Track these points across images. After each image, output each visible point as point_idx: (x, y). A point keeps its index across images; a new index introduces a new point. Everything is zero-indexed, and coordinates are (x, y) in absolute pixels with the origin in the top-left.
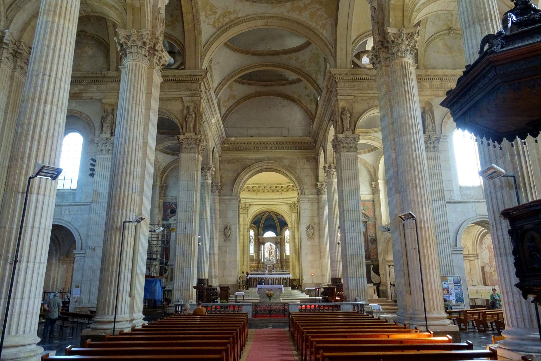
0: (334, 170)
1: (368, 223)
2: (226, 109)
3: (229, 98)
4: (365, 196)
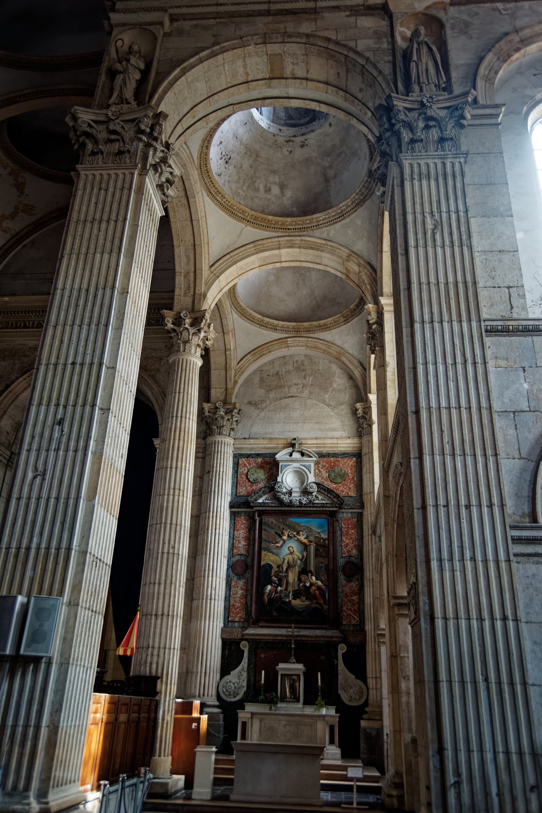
0: (192, 330)
1: (340, 515)
2: (8, 236)
3: (17, 209)
4: (335, 441)
